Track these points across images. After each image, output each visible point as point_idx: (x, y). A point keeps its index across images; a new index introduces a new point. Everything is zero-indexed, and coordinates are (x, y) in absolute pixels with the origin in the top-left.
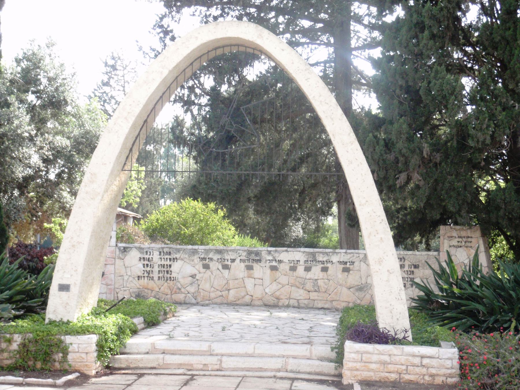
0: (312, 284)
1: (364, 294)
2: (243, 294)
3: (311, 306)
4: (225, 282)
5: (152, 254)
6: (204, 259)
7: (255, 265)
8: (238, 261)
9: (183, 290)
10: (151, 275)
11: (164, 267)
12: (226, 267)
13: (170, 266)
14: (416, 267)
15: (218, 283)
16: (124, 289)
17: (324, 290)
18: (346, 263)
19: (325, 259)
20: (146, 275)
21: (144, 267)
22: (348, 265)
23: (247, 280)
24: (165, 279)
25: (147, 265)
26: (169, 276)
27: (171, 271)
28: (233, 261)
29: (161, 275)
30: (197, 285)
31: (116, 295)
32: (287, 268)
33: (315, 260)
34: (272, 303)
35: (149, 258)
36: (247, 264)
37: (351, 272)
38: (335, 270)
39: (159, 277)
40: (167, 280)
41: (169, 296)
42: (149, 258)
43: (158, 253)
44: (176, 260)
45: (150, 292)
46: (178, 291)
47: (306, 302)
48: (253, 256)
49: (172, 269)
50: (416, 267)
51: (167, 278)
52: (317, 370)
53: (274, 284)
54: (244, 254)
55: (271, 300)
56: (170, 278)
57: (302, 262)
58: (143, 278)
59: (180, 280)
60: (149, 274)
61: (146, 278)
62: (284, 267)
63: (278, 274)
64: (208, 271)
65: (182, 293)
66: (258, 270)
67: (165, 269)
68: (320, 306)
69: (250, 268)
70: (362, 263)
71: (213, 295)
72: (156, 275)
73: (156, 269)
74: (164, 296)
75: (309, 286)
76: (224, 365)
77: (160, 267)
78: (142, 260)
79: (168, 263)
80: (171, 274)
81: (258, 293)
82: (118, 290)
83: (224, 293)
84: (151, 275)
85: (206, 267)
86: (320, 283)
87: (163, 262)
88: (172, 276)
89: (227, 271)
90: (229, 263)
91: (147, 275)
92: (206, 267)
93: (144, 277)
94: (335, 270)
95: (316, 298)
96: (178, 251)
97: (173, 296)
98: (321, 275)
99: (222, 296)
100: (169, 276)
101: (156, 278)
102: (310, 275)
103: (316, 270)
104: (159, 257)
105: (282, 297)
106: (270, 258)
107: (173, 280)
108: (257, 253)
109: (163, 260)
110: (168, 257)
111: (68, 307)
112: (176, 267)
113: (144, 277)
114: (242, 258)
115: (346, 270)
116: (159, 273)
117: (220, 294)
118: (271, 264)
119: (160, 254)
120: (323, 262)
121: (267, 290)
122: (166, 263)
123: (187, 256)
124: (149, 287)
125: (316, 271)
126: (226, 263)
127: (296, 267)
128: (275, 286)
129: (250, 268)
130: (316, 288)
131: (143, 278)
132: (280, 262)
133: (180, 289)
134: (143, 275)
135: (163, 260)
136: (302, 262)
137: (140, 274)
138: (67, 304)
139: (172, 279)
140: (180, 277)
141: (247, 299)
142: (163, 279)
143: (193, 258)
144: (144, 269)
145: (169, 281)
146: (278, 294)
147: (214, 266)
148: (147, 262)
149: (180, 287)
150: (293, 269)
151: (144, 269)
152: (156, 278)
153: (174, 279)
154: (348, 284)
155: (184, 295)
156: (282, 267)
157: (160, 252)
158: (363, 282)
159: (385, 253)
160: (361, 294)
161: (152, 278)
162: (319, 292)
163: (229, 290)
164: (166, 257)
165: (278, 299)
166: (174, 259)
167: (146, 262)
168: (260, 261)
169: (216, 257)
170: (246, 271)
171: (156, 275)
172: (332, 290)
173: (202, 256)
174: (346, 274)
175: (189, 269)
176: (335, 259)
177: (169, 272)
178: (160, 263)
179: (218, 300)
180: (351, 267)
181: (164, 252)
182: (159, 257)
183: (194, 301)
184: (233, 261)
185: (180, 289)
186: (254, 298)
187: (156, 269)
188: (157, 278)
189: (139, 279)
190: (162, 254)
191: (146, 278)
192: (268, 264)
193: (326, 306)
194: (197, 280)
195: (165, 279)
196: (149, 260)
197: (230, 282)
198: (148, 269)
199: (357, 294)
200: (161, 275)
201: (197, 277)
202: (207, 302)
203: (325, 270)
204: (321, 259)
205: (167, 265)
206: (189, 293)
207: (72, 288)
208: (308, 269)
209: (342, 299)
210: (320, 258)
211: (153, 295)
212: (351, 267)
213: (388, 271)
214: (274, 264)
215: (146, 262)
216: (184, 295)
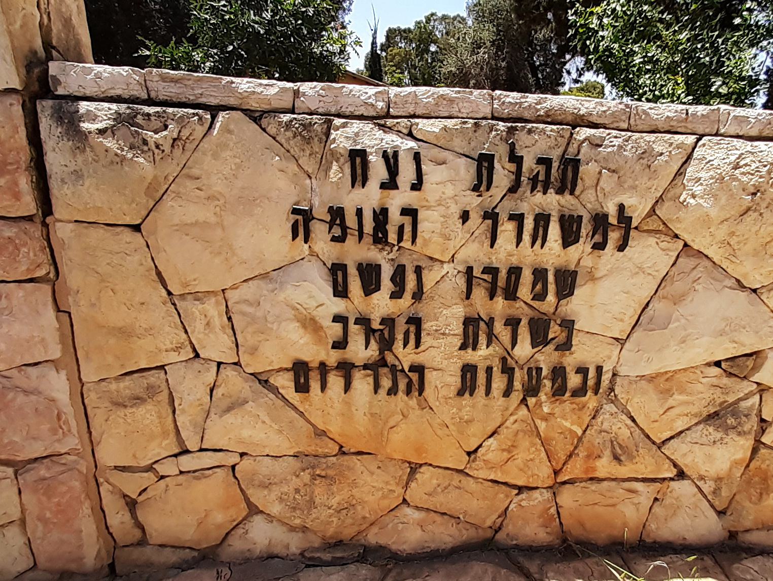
5: (407, 173)
10: (405, 355)
11: (511, 294)
13: (567, 282)
16: (186, 462)
20: (360, 350)
21: (341, 291)
24: (519, 377)
25: (370, 277)
26: (546, 359)
27: (568, 325)
29: (483, 355)
31: (118, 518)
35: (381, 216)
39: (468, 370)
40: (532, 390)
42: (381, 216)
43: (466, 171)
44: (614, 236)
49: (577, 305)
51: (535, 372)
56: (559, 373)
58: (335, 381)
60: (386, 344)
61: (362, 383)
67: (520, 309)
72: (441, 354)
73: (446, 315)
77: (479, 293)
78: (320, 230)
79: (553, 252)
80: (566, 346)
82: (131, 485)
84: (405, 355)
87: (507, 250)
88: (570, 361)
91: (373, 351)
93: (346, 369)
97: (567, 498)
100: (546, 359)
101: (443, 380)
107: (580, 392)
109: (507, 229)
110: (551, 201)
112: (609, 295)
113: (346, 369)
116: (469, 342)
122: (528, 255)
131: (335, 381)
134: (333, 357)
135: (507, 229)
137: (315, 352)
139: (574, 380)
140: (632, 363)
142: (499, 383)
144: (338, 306)
148: (367, 248)
151: (338, 306)
152: (443, 380)
153: (593, 382)
157: (485, 163)
164: (534, 202)
166: (600, 221)
167: (356, 252)
171: (441, 354)
177: (554, 331)
178: (475, 252)
181: (516, 159)
187: (446, 315)
188: (455, 381)
189: (302, 388)
190: (502, 175)
191: (362, 383)
194: (762, 389)
195: (519, 377)
196: (380, 238)
198: (381, 304)
205: (540, 274)
206: (681, 475)
215: (356, 252)
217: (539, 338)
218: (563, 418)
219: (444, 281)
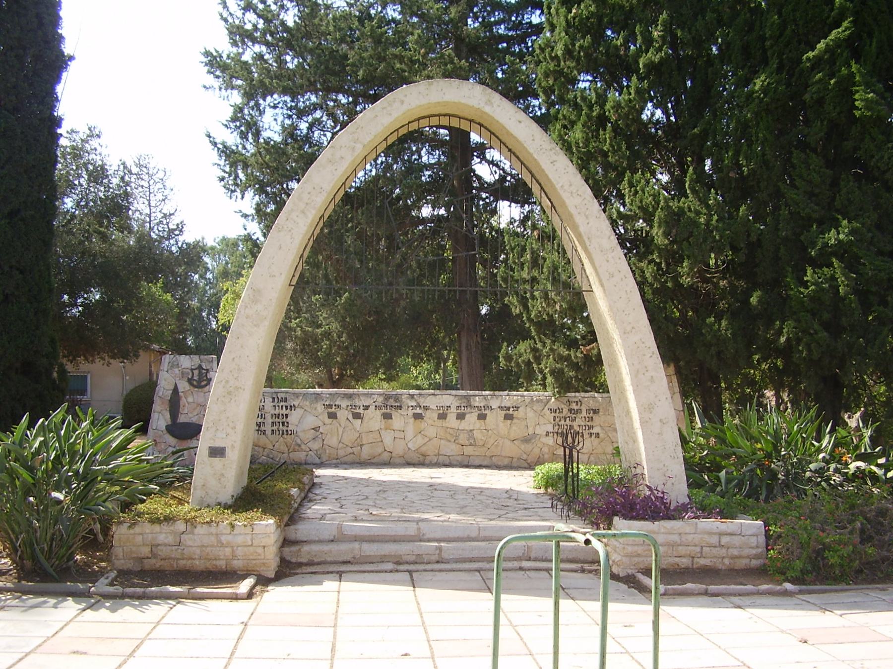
0: (466, 435)
1: (531, 448)
2: (380, 450)
3: (466, 463)
4: (358, 435)
6: (330, 406)
7: (395, 414)
8: (372, 408)
9: (303, 447)
10: (262, 428)
12: (357, 416)
13: (287, 416)
14: (596, 412)
15: (349, 437)
17: (481, 443)
18: (508, 409)
19: (482, 405)
22: (511, 412)
23: (383, 433)
26: (285, 428)
28: (366, 408)
29: (275, 428)
30: (320, 441)
32: (435, 416)
33: (469, 405)
34: (416, 460)
36: (384, 410)
37: (515, 421)
38: (495, 418)
41: (286, 455)
43: (271, 400)
45: (261, 450)
46: (297, 447)
47: (459, 458)
48: (391, 402)
50: (596, 412)
52: (570, 557)
53: (419, 437)
54: (381, 399)
55: (415, 458)
57: (453, 409)
59: (300, 434)
62: (431, 416)
63: (423, 425)
64: (335, 421)
65: (302, 450)
66: (398, 420)
67: (280, 420)
68: (477, 462)
69: (387, 417)
70: (529, 409)
71: (341, 453)
73: (269, 420)
74: (280, 455)
75: (463, 438)
76: (445, 555)
79: (284, 412)
81: (399, 449)
83: (355, 450)
84: (262, 428)
85: (332, 416)
86: (477, 434)
87: (277, 412)
88: (289, 429)
89: (360, 421)
90: (361, 411)
92: (332, 416)
94: (495, 418)
95: (472, 453)
96: (297, 395)
98: (479, 424)
99: (353, 453)
100: (285, 428)
101: (269, 432)
102: (464, 425)
103: (472, 418)
104: (272, 404)
105: (429, 453)
106: (414, 404)
108: (397, 398)
110: (283, 404)
111: (223, 479)
112: (294, 417)
114: (377, 404)
115: (508, 417)
116: (272, 426)
117: (351, 450)
118: (414, 411)
119: (273, 401)
120: (479, 408)
121: (410, 445)
123: (308, 403)
124: (261, 444)
125: (472, 418)
126: (358, 411)
127: (446, 414)
128: (420, 441)
129: (387, 417)
130: (472, 441)
132: (426, 408)
133: (300, 446)
136: (453, 409)
138: (222, 475)
141: (386, 456)
143: (315, 405)
145: (285, 436)
146: (424, 449)
147: (343, 415)
149: (299, 442)
150: (442, 416)
152: (269, 432)
154: (512, 437)
155: (305, 453)
156: (428, 414)
158: (531, 431)
159: (656, 397)
160: (527, 447)
161: (264, 433)
162: (475, 445)
163: (361, 446)
164: (282, 404)
165: (424, 456)
168: (400, 407)
169: (344, 403)
170: (383, 421)
171: (268, 428)
172: (491, 443)
173: (327, 403)
174: (509, 422)
175: (311, 421)
176: (495, 404)
178: (273, 412)
179: (349, 459)
180: (515, 413)
182: (272, 404)
183: (317, 461)
184: (366, 408)
185: (300, 446)
186: (394, 455)
187: (269, 420)
190: (276, 400)
192: (411, 412)
193: (485, 463)
197: (363, 435)
199: (523, 447)
200: (275, 428)
201: (321, 430)
202: (335, 461)
203: (482, 417)
204: (477, 404)
207: (228, 452)
208: (461, 417)
209: (503, 454)
210: (477, 402)
211: (265, 453)
212: (515, 413)
213: (661, 420)
214: (418, 411)
216: (305, 453)
217: (283, 425)
218: (288, 438)
219: (268, 416)
